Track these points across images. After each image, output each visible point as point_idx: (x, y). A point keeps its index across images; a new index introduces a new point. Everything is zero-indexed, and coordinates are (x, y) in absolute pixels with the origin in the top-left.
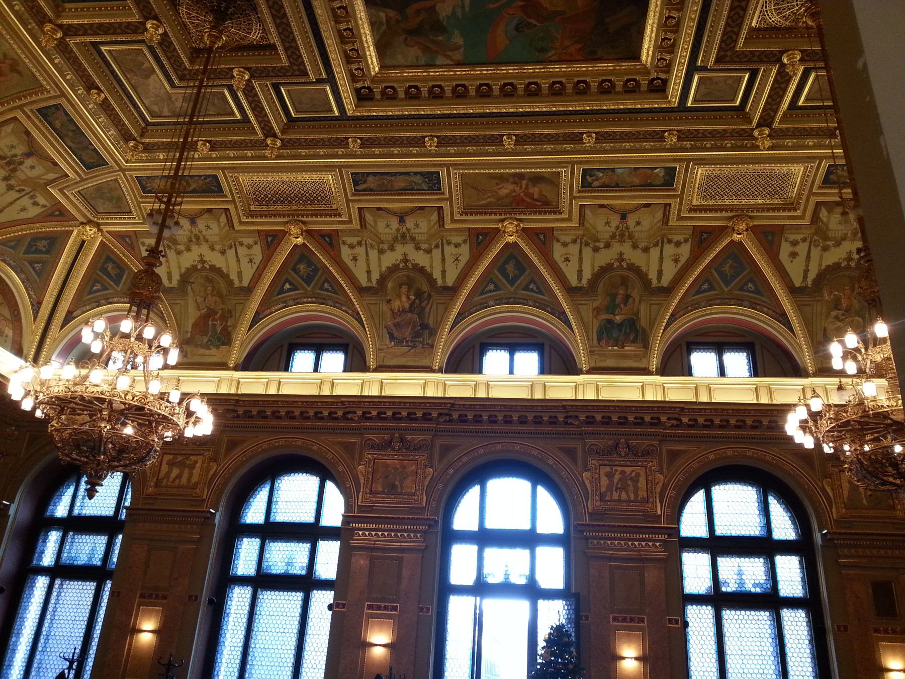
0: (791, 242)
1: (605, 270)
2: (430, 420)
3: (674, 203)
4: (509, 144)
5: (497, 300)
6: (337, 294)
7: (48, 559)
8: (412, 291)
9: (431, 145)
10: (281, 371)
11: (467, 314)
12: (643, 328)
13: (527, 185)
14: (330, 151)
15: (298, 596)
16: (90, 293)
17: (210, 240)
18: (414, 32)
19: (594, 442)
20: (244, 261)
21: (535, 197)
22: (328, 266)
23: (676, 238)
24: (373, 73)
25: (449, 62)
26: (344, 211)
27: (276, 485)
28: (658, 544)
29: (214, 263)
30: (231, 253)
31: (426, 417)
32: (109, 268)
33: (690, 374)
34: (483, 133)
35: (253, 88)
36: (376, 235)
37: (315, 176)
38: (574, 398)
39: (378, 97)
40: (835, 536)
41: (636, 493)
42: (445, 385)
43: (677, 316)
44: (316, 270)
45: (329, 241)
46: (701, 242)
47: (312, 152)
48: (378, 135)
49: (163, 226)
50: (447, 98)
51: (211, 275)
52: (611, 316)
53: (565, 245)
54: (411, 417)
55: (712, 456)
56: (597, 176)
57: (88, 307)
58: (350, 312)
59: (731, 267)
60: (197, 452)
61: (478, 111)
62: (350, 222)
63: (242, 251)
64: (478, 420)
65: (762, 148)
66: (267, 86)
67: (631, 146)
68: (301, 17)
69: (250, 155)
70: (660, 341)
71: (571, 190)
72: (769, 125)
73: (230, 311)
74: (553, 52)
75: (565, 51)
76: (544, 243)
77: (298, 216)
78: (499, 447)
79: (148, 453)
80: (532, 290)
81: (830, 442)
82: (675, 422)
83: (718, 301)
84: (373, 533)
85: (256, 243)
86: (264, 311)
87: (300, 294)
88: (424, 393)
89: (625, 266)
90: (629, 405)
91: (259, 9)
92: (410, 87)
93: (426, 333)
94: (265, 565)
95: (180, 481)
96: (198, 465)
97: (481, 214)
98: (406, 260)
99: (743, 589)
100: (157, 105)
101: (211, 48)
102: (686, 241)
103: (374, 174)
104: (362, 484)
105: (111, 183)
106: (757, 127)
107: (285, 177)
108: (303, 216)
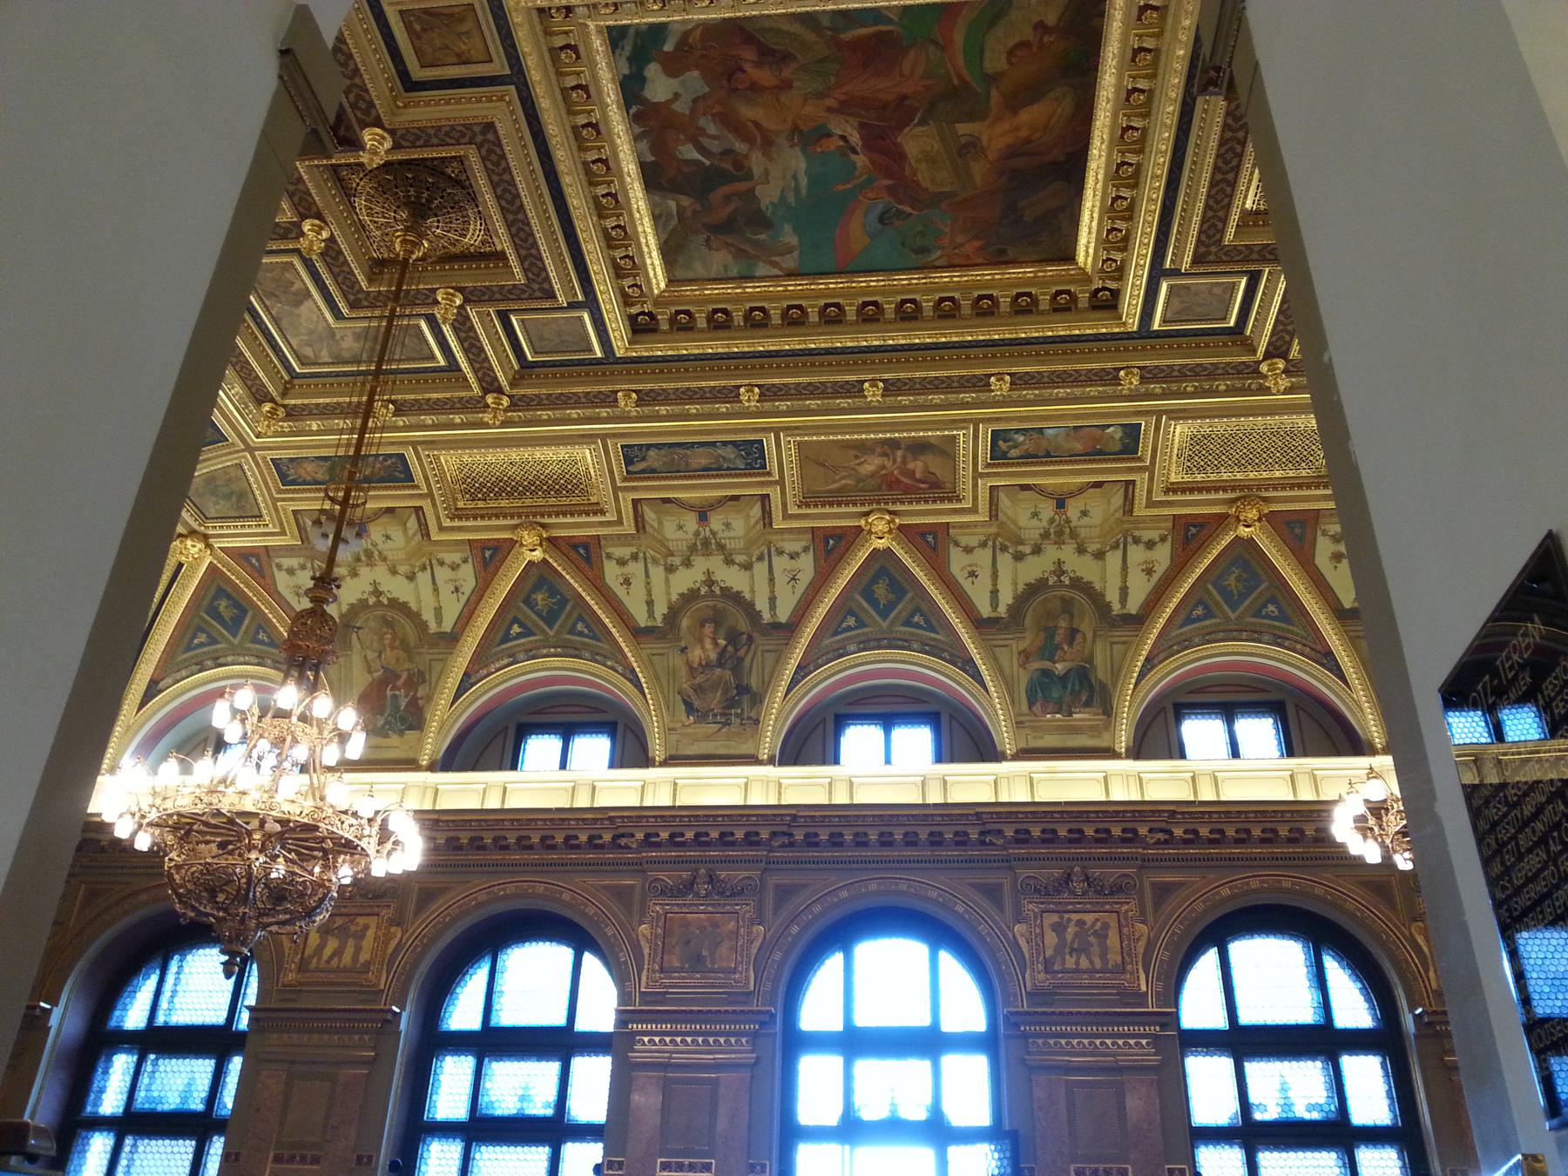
0: (1333, 536)
1: (1035, 589)
2: (758, 843)
3: (1141, 480)
4: (873, 394)
5: (861, 642)
6: (598, 640)
7: (111, 1101)
8: (722, 632)
9: (749, 399)
10: (505, 769)
11: (812, 668)
12: (1101, 682)
13: (904, 457)
14: (588, 412)
15: (542, 1153)
16: (188, 649)
17: (390, 557)
19: (1031, 873)
20: (446, 590)
21: (918, 475)
22: (584, 594)
23: (1147, 535)
24: (656, 291)
25: (776, 272)
26: (610, 505)
27: (499, 964)
28: (1144, 1042)
29: (395, 595)
30: (424, 578)
31: (751, 840)
32: (222, 608)
33: (1183, 756)
34: (832, 379)
35: (468, 318)
36: (663, 545)
37: (563, 453)
38: (993, 800)
39: (665, 326)
40: (1434, 1018)
41: (1104, 959)
42: (780, 785)
43: (1156, 661)
44: (563, 602)
45: (585, 553)
46: (1187, 540)
47: (558, 414)
48: (665, 386)
49: (338, 539)
50: (775, 327)
51: (390, 614)
52: (1047, 665)
53: (968, 550)
54: (725, 840)
55: (1226, 892)
56: (1014, 440)
57: (184, 673)
58: (620, 669)
59: (1238, 580)
60: (368, 911)
61: (823, 345)
62: (620, 522)
63: (442, 574)
64: (836, 841)
65: (1274, 391)
66: (489, 313)
67: (1068, 394)
68: (545, 211)
69: (458, 420)
70: (1131, 702)
71: (975, 464)
72: (1284, 355)
73: (421, 673)
74: (939, 253)
76: (934, 549)
77: (534, 516)
78: (873, 886)
79: (322, 900)
80: (918, 626)
81: (1405, 850)
82: (1161, 836)
83: (1221, 635)
84: (668, 1039)
85: (465, 561)
86: (477, 671)
87: (536, 641)
88: (745, 798)
90: (1084, 809)
91: (480, 200)
92: (715, 311)
93: (746, 698)
94: (483, 1100)
95: (340, 962)
96: (370, 933)
97: (831, 504)
98: (710, 582)
99: (1291, 1115)
100: (311, 345)
101: (406, 260)
102: (1163, 539)
103: (658, 446)
104: (646, 956)
105: (231, 470)
106: (1264, 360)
107: (514, 454)
108: (542, 515)
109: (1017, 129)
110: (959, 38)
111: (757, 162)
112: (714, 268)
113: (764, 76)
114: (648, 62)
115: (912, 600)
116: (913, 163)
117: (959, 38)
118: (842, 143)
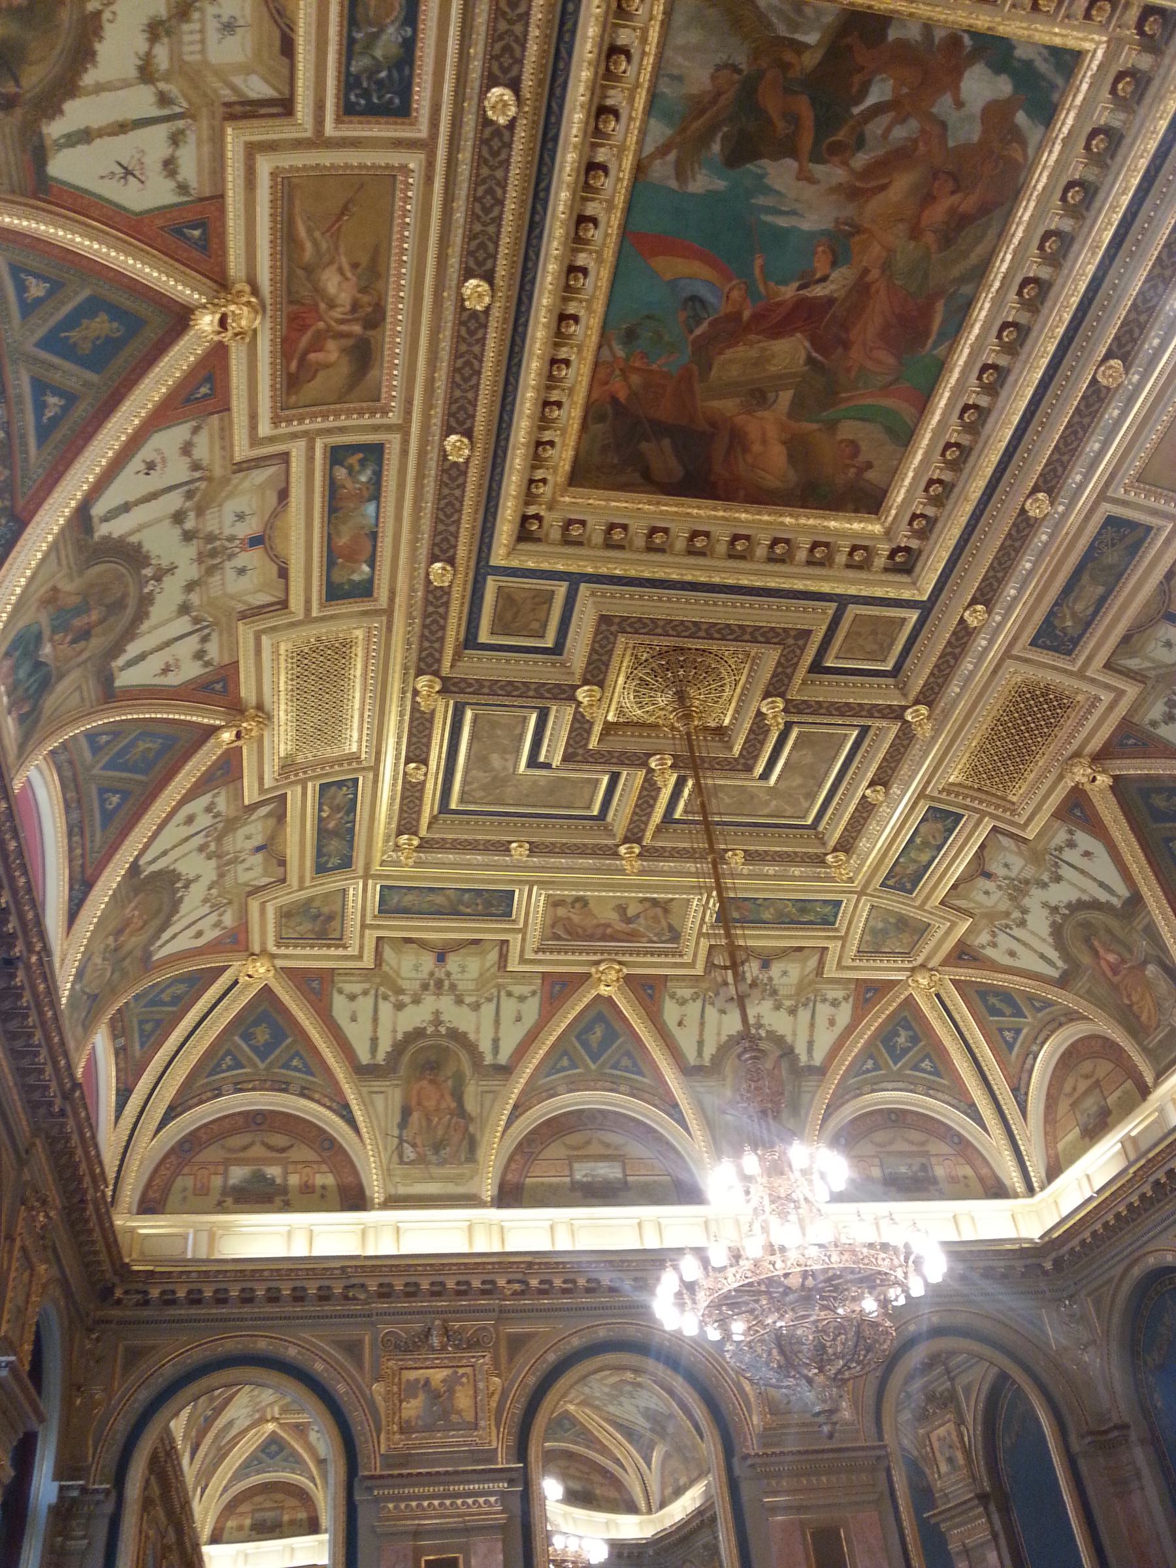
18: (749, 88)
21: (312, 356)
25: (649, 149)
52: (47, 633)
56: (359, 472)
74: (620, 353)
75: (617, 372)
80: (40, 407)
89: (146, 590)
109: (764, 442)
111: (832, 173)
112: (680, 60)
113: (937, 213)
114: (1017, 87)
115: (87, 384)
118: (818, 276)
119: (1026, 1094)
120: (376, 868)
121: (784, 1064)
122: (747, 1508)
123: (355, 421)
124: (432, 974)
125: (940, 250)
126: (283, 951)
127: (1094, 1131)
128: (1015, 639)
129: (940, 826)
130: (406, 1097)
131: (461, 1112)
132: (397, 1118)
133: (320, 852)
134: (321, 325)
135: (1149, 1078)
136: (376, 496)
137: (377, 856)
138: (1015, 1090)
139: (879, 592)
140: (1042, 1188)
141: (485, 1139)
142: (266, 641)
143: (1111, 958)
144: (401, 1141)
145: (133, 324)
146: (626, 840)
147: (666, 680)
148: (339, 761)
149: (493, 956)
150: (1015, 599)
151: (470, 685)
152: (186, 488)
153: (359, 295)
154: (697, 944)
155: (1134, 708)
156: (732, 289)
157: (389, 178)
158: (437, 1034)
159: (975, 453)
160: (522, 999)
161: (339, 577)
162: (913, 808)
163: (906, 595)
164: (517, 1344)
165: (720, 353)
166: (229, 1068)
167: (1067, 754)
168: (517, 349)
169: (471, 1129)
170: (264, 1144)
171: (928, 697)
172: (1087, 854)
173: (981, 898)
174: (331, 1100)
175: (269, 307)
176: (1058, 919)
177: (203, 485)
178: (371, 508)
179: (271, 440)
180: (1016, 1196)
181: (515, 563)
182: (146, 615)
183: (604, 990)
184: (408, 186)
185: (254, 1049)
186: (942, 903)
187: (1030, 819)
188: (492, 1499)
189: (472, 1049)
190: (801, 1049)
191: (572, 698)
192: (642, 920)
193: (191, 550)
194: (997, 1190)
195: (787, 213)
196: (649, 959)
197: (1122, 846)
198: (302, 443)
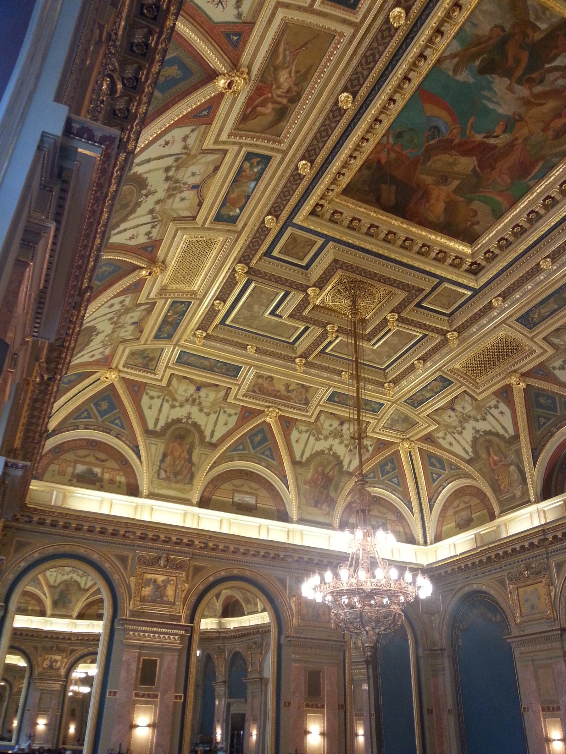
18: (504, 41)
21: (259, 109)
25: (447, 53)
56: (255, 167)
74: (391, 141)
75: (386, 149)
89: (140, 200)
109: (437, 199)
110: (499, 199)
111: (523, 91)
112: (480, 16)
116: (456, 157)
117: (499, 199)
118: (495, 134)
119: (435, 502)
120: (182, 342)
121: (337, 468)
122: (284, 658)
123: (265, 143)
124: (192, 395)
125: (552, 140)
126: (125, 369)
127: (464, 526)
128: (510, 316)
129: (441, 384)
130: (166, 448)
131: (190, 461)
132: (160, 458)
133: (159, 330)
134: (270, 95)
135: (497, 512)
136: (257, 180)
137: (185, 337)
138: (430, 500)
139: (460, 280)
140: (431, 544)
141: (198, 475)
142: (179, 233)
143: (496, 458)
144: (160, 468)
145: (187, 72)
146: (301, 356)
147: (350, 293)
148: (187, 293)
149: (222, 393)
150: (518, 300)
151: (261, 273)
152: (177, 156)
153: (292, 86)
154: (316, 408)
155: (547, 360)
156: (454, 128)
157: (331, 36)
158: (187, 422)
159: (528, 233)
160: (230, 415)
161: (222, 212)
162: (433, 374)
163: (471, 285)
164: (197, 570)
165: (437, 155)
166: (85, 418)
167: (511, 370)
168: (350, 129)
169: (193, 469)
170: (94, 456)
171: (460, 330)
172: (502, 413)
173: (446, 418)
174: (130, 442)
175: (252, 81)
176: (478, 436)
177: (184, 156)
178: (253, 184)
179: (224, 143)
180: (419, 544)
181: (305, 225)
182: (135, 211)
183: (268, 420)
184: (339, 42)
185: (99, 411)
186: (428, 415)
187: (482, 392)
188: (177, 637)
189: (201, 433)
190: (345, 463)
191: (305, 291)
192: (295, 392)
193: (166, 186)
194: (411, 540)
195: (495, 103)
196: (292, 410)
197: (519, 414)
198: (236, 148)
